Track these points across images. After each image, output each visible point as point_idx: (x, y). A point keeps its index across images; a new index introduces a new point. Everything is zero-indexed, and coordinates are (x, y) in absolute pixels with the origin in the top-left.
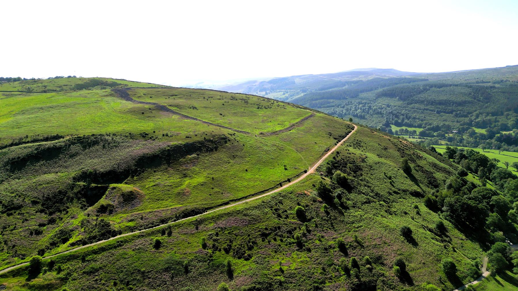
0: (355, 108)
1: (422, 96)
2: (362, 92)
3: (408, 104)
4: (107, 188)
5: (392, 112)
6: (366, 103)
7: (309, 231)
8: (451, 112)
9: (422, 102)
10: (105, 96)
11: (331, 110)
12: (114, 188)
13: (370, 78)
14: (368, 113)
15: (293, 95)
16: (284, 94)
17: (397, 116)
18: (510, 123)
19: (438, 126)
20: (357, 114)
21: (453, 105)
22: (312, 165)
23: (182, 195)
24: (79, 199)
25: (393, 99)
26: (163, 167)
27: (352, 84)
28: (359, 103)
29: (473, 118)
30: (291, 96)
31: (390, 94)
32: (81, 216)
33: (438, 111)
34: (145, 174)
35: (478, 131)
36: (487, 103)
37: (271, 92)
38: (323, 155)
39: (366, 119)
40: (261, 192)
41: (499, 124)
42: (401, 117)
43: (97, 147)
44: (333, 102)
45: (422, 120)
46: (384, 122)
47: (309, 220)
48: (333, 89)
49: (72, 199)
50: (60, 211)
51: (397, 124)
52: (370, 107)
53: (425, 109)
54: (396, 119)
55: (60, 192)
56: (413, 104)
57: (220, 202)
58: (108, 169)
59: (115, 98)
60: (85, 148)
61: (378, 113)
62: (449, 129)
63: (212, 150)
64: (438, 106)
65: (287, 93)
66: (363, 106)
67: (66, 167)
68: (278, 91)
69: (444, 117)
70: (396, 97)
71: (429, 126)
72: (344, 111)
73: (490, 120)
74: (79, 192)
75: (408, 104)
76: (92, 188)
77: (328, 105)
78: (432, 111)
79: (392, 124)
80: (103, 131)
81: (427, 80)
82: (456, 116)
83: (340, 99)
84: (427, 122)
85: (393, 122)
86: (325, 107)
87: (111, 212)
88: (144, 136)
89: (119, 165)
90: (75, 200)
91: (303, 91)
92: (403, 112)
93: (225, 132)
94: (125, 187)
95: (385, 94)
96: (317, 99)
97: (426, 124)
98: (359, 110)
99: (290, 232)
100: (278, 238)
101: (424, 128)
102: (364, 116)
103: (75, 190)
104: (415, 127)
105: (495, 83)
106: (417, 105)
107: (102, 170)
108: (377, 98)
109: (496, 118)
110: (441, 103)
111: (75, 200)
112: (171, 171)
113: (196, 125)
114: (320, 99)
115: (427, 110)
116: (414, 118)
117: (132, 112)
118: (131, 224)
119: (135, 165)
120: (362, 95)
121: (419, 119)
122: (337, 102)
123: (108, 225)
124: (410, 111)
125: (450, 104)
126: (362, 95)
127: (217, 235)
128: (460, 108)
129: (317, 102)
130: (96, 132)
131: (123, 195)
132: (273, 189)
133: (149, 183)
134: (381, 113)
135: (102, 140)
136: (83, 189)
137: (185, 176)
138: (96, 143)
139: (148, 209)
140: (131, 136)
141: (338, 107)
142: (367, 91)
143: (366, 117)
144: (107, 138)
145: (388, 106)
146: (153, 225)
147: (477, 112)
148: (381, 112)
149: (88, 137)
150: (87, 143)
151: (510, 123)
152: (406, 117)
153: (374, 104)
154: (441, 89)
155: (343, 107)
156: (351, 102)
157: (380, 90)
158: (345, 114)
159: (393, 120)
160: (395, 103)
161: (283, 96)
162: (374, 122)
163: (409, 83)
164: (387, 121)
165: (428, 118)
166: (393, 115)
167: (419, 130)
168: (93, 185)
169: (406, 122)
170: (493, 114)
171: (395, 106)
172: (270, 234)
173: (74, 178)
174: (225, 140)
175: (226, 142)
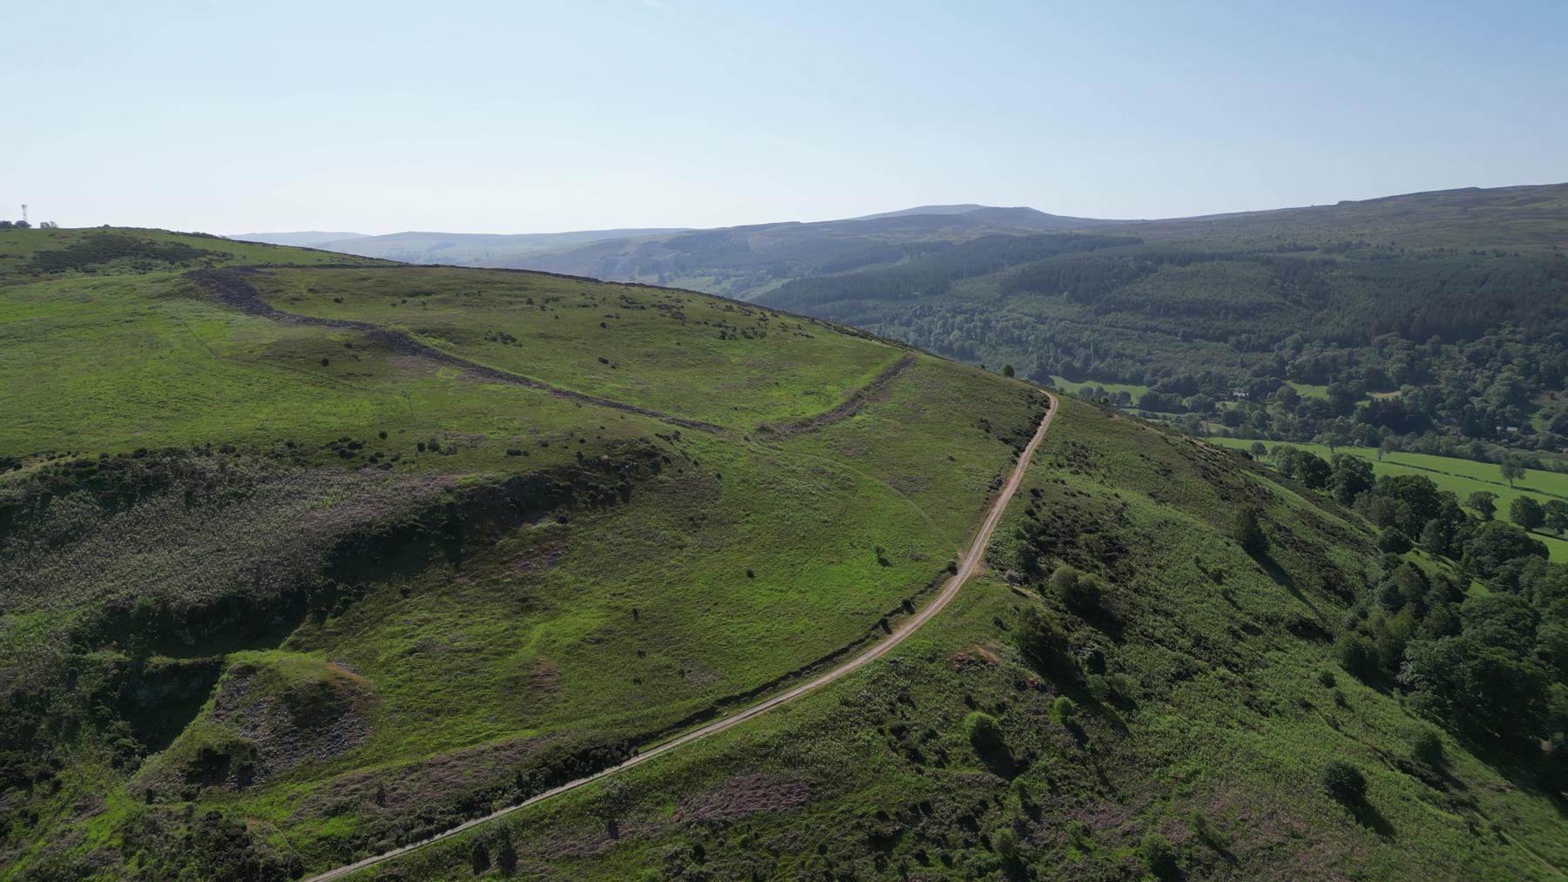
0: (944, 325)
2: (957, 276)
3: (1097, 313)
4: (214, 671)
5: (1052, 339)
6: (974, 311)
7: (1034, 812)
8: (1223, 338)
9: (1138, 307)
10: (162, 296)
12: (249, 670)
13: (974, 234)
14: (982, 341)
16: (718, 282)
17: (1068, 351)
18: (1392, 368)
19: (1190, 379)
20: (950, 344)
21: (1226, 315)
22: (966, 540)
23: (525, 689)
24: (102, 724)
26: (436, 573)
28: (956, 311)
29: (1287, 353)
31: (1044, 283)
32: (119, 802)
34: (369, 605)
35: (1304, 391)
36: (1320, 308)
38: (989, 502)
40: (822, 661)
41: (1363, 371)
42: (1081, 353)
43: (160, 502)
45: (1142, 362)
46: (1034, 367)
47: (1023, 766)
48: (867, 268)
49: (75, 724)
50: (25, 783)
51: (1072, 375)
52: (987, 322)
53: (1146, 329)
54: (1067, 359)
55: (19, 699)
56: (1113, 314)
57: (681, 708)
58: (217, 590)
59: (200, 305)
60: (110, 505)
61: (1011, 341)
62: (1221, 387)
63: (610, 500)
64: (1185, 319)
65: (728, 277)
66: (967, 321)
67: (37, 589)
69: (1202, 351)
70: (1061, 292)
71: (1166, 380)
72: (912, 336)
73: (1334, 359)
74: (101, 695)
75: (1097, 313)
76: (154, 674)
77: (861, 316)
79: (1057, 374)
80: (180, 435)
81: (1140, 241)
82: (1239, 347)
84: (1159, 366)
87: (246, 777)
88: (347, 450)
89: (258, 571)
90: (86, 732)
91: (778, 274)
92: (1086, 336)
93: (647, 428)
94: (295, 664)
96: (825, 300)
97: (1155, 372)
98: (956, 332)
99: (968, 822)
100: (933, 852)
101: (1150, 384)
103: (84, 688)
104: (1124, 381)
105: (1329, 251)
106: (1124, 317)
107: (190, 596)
109: (1351, 354)
110: (1192, 310)
111: (86, 732)
112: (470, 588)
113: (530, 402)
115: (1154, 330)
116: (1119, 356)
117: (282, 356)
118: (338, 827)
119: (327, 572)
121: (1132, 357)
123: (239, 839)
125: (1218, 314)
126: (962, 286)
127: (699, 854)
128: (1247, 324)
129: (828, 306)
130: (150, 438)
131: (291, 699)
132: (861, 644)
133: (389, 643)
134: (1019, 341)
135: (179, 473)
136: (115, 682)
137: (527, 606)
138: (153, 484)
139: (395, 754)
140: (296, 453)
141: (891, 322)
143: (977, 353)
144: (199, 462)
145: (1041, 319)
146: (432, 824)
147: (1297, 336)
148: (1020, 337)
149: (121, 464)
150: (121, 486)
151: (1392, 368)
152: (1096, 351)
153: (999, 314)
154: (1188, 268)
155: (908, 324)
156: (930, 308)
157: (1010, 271)
159: (1057, 360)
160: (1060, 310)
164: (1041, 366)
166: (1058, 345)
168: (159, 660)
170: (1343, 342)
172: (898, 835)
173: (76, 637)
174: (650, 459)
175: (656, 468)
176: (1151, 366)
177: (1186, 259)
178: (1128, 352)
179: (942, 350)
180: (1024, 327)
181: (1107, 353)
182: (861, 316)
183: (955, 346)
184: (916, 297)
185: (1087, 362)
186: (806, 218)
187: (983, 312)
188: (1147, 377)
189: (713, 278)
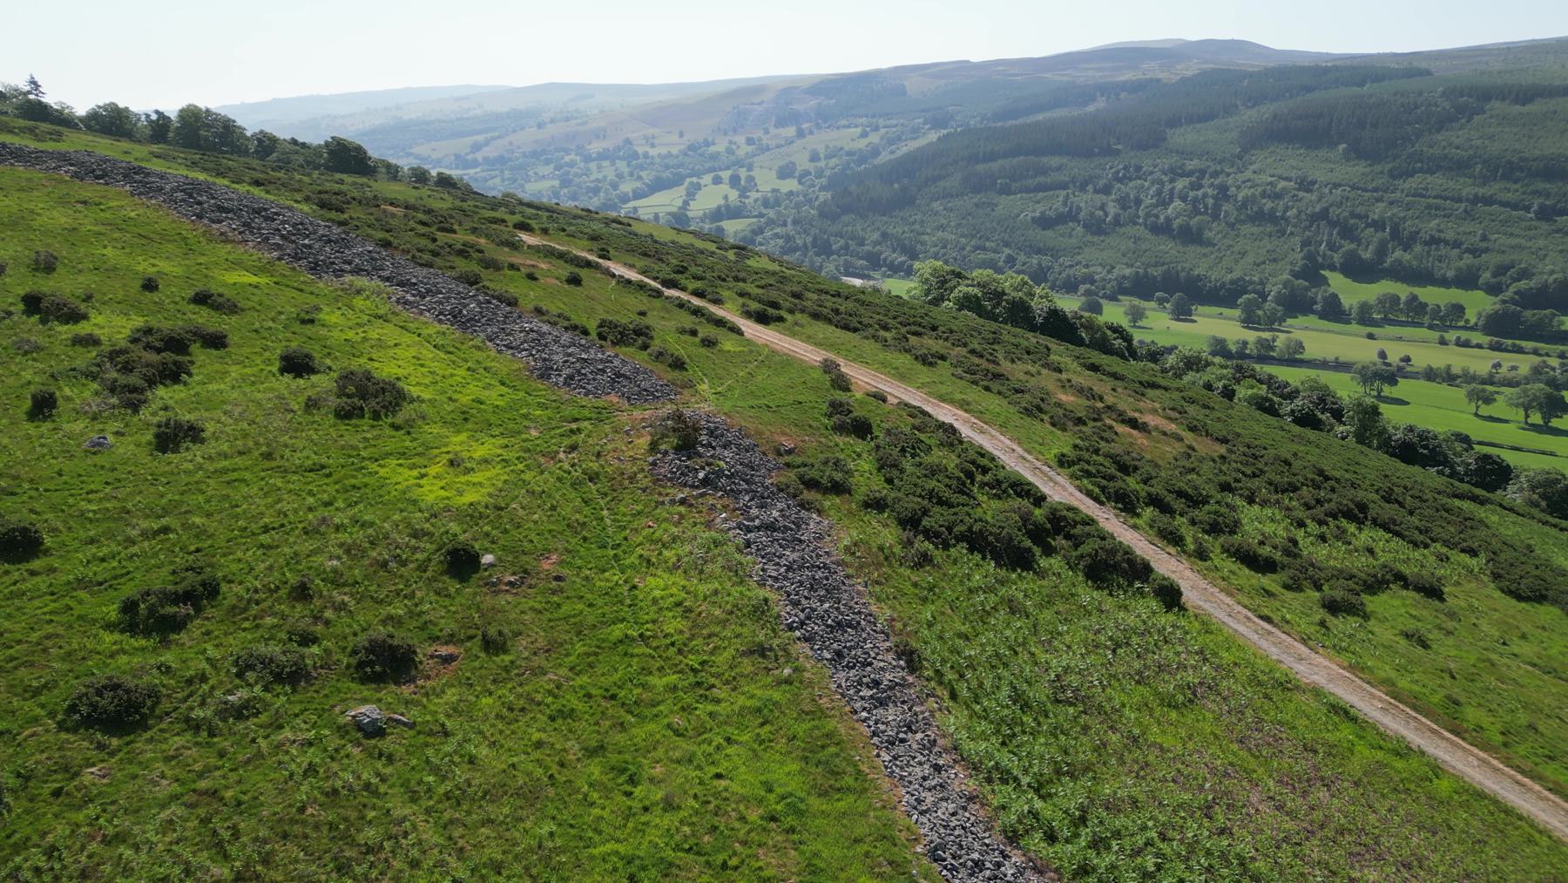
0: (1159, 193)
1: (1458, 139)
2: (1174, 122)
3: (1393, 175)
6: (1203, 172)
9: (1459, 167)
11: (1055, 203)
13: (1189, 69)
15: (899, 139)
16: (864, 135)
17: (1348, 233)
20: (1168, 220)
25: (1322, 153)
27: (1123, 95)
28: (1176, 173)
30: (891, 142)
31: (1308, 131)
33: (1542, 208)
37: (818, 127)
39: (1210, 243)
42: (1373, 238)
44: (1059, 168)
45: (1475, 252)
46: (1298, 257)
48: (1048, 115)
51: (1359, 271)
52: (1223, 189)
53: (1476, 200)
54: (1348, 246)
56: (1418, 178)
61: (1260, 217)
64: (1541, 185)
65: (876, 129)
66: (1196, 186)
68: (844, 122)
70: (1333, 145)
71: (1523, 285)
72: (1112, 209)
75: (1393, 175)
77: (1041, 179)
78: (1515, 207)
79: (1332, 268)
81: (1428, 73)
83: (1088, 154)
84: (1507, 259)
85: (1337, 258)
86: (1028, 190)
91: (937, 124)
92: (1378, 211)
95: (1281, 133)
96: (992, 157)
97: (1501, 270)
98: (1178, 203)
101: (1493, 290)
102: (1200, 231)
104: (1444, 283)
106: (1438, 181)
108: (1245, 150)
114: (1005, 156)
115: (1488, 201)
116: (1434, 241)
120: (1182, 137)
121: (1456, 244)
122: (1077, 167)
124: (1408, 207)
126: (1182, 137)
129: (995, 166)
134: (1271, 218)
141: (1083, 188)
142: (1192, 119)
143: (1208, 234)
145: (1306, 185)
148: (1273, 210)
152: (1395, 234)
153: (1241, 177)
155: (1106, 190)
157: (1249, 116)
158: (1117, 222)
159: (1332, 247)
160: (1332, 170)
161: (862, 144)
162: (1250, 259)
163: (1361, 84)
164: (1310, 257)
165: (1503, 240)
166: (1333, 224)
167: (1478, 304)
169: (1399, 261)
171: (1336, 186)
176: (1493, 259)
177: (1525, 95)
178: (1450, 235)
179: (1156, 229)
180: (1278, 196)
181: (1413, 237)
182: (1041, 179)
183: (1176, 224)
184: (1118, 152)
185: (1382, 252)
186: (976, 57)
187: (1215, 174)
188: (1486, 276)
189: (859, 130)
